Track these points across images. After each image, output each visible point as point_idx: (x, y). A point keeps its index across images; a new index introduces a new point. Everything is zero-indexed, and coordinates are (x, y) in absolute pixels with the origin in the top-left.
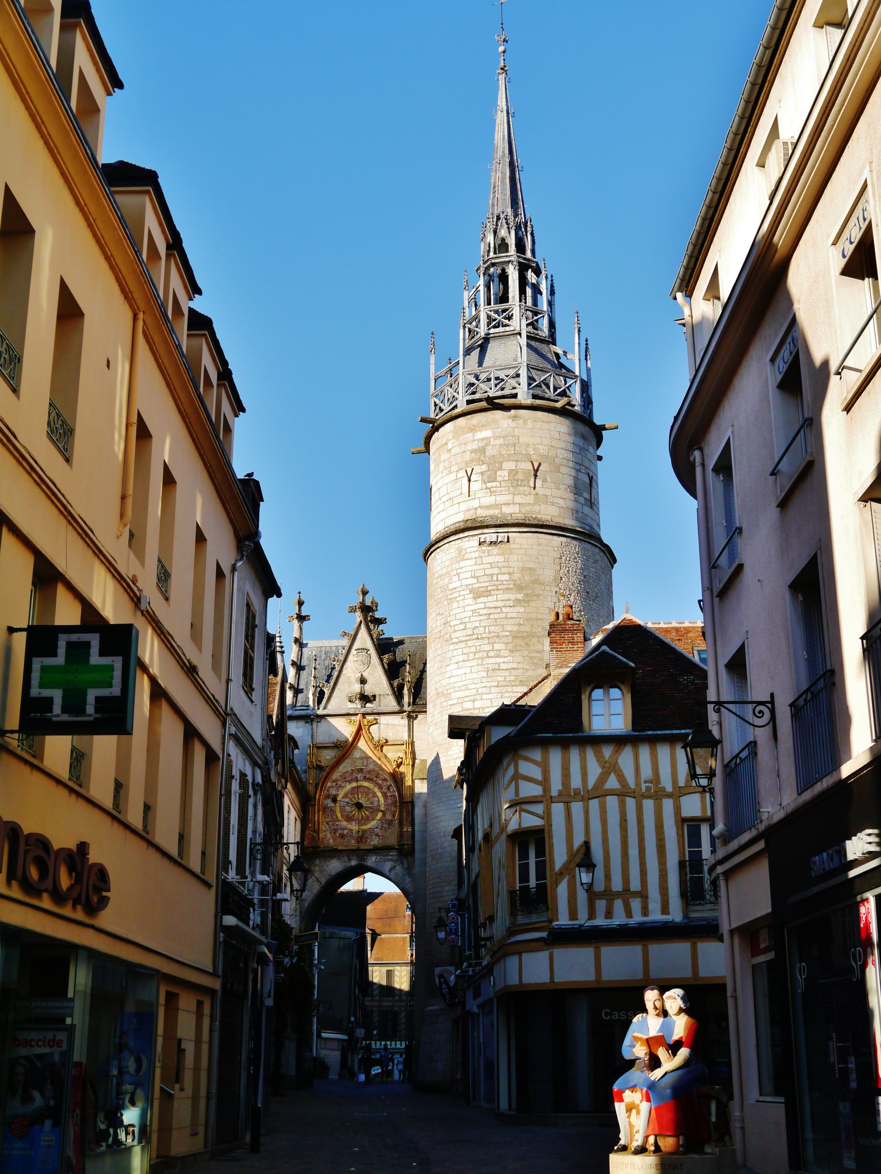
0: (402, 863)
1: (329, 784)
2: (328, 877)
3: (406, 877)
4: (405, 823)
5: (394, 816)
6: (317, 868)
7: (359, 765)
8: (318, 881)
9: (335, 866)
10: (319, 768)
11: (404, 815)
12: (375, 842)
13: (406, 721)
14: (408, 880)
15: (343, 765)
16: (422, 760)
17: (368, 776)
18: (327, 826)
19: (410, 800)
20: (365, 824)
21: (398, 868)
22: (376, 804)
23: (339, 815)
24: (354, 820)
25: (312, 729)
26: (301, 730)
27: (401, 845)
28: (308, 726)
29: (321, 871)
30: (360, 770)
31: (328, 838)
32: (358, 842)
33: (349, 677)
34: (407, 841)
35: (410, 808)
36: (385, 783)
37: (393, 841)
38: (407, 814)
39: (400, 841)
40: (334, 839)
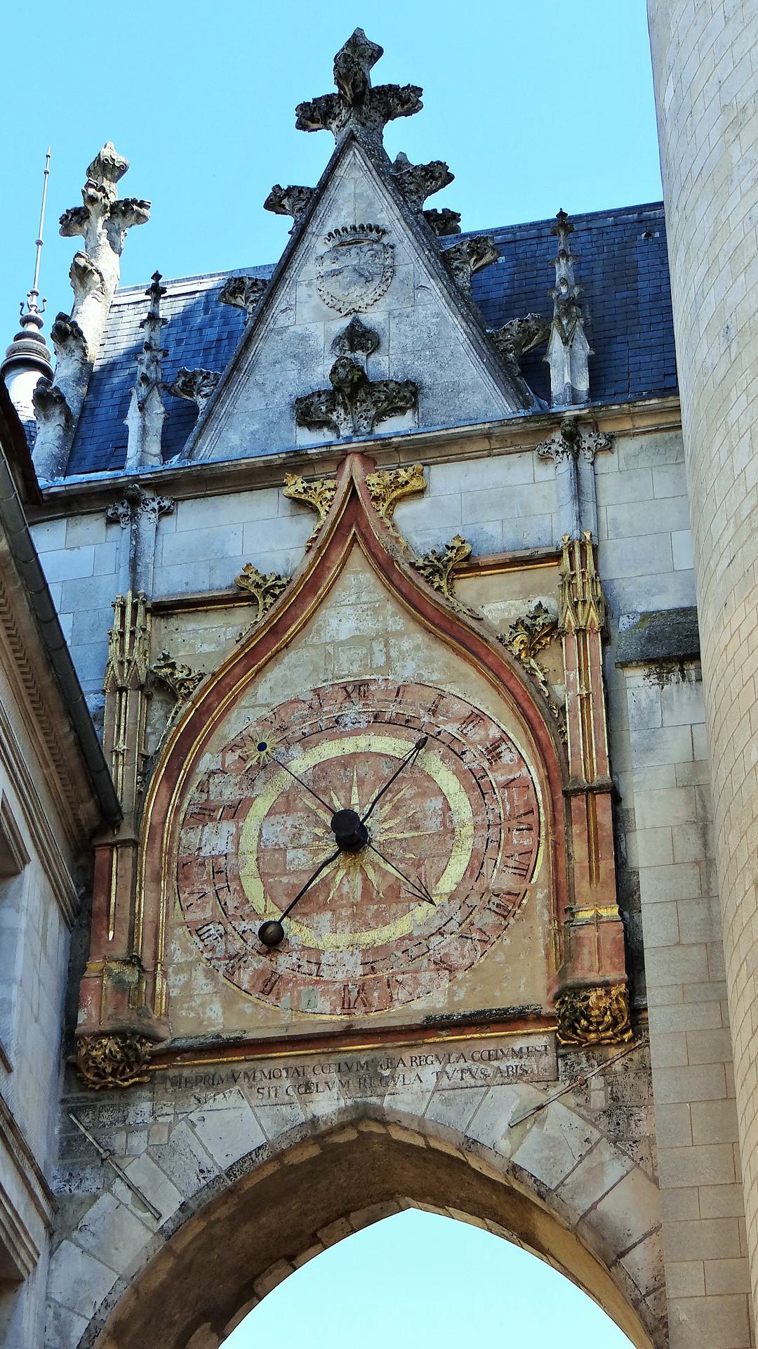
0: (581, 1087)
1: (208, 762)
2: (195, 1183)
3: (606, 1152)
4: (583, 887)
5: (524, 872)
6: (138, 1142)
7: (349, 667)
8: (145, 1205)
9: (233, 1127)
10: (161, 686)
11: (579, 850)
12: (435, 998)
13: (565, 465)
14: (614, 1170)
15: (275, 674)
16: (646, 616)
17: (392, 710)
18: (195, 944)
19: (601, 776)
20: (382, 919)
21: (560, 1113)
22: (433, 825)
23: (254, 889)
24: (324, 907)
25: (136, 535)
26: (87, 552)
27: (569, 992)
28: (120, 535)
29: (158, 1155)
30: (360, 689)
31: (197, 1001)
32: (347, 1006)
33: (303, 338)
34: (599, 965)
35: (605, 818)
36: (476, 734)
37: (529, 984)
38: (593, 842)
39: (562, 974)
40: (228, 1004)
